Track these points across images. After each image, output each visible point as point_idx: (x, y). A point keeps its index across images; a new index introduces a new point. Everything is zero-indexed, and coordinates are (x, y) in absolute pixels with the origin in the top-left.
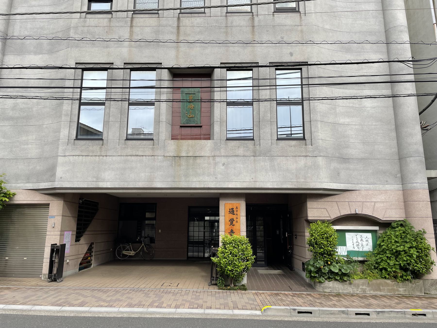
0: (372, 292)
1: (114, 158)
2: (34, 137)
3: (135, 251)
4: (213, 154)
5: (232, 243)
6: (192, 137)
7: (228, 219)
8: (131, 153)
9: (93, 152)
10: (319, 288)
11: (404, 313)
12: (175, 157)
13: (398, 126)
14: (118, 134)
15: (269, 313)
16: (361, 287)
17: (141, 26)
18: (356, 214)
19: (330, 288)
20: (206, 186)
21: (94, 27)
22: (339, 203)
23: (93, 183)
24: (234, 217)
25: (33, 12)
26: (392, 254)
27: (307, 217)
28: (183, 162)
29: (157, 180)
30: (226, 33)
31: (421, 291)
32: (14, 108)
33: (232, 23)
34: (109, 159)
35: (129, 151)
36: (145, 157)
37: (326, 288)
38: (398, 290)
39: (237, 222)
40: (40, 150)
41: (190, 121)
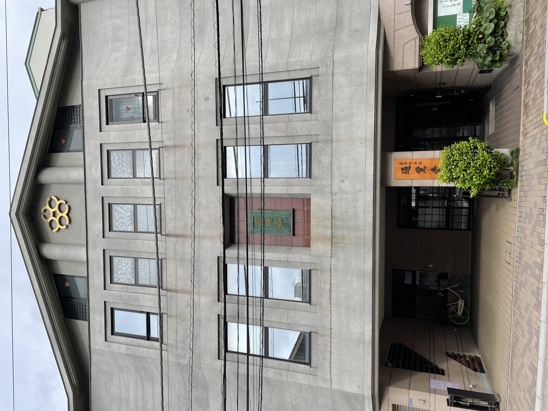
3: (458, 300)
4: (329, 195)
5: (450, 170)
7: (417, 175)
8: (328, 298)
10: (517, 49)
12: (332, 243)
17: (176, 280)
18: (411, 3)
22: (397, 28)
23: (366, 348)
24: (413, 167)
27: (414, 69)
28: (339, 233)
30: (183, 178)
33: (171, 172)
34: (335, 326)
35: (325, 300)
36: (332, 281)
37: (516, 39)
39: (420, 163)
41: (287, 223)
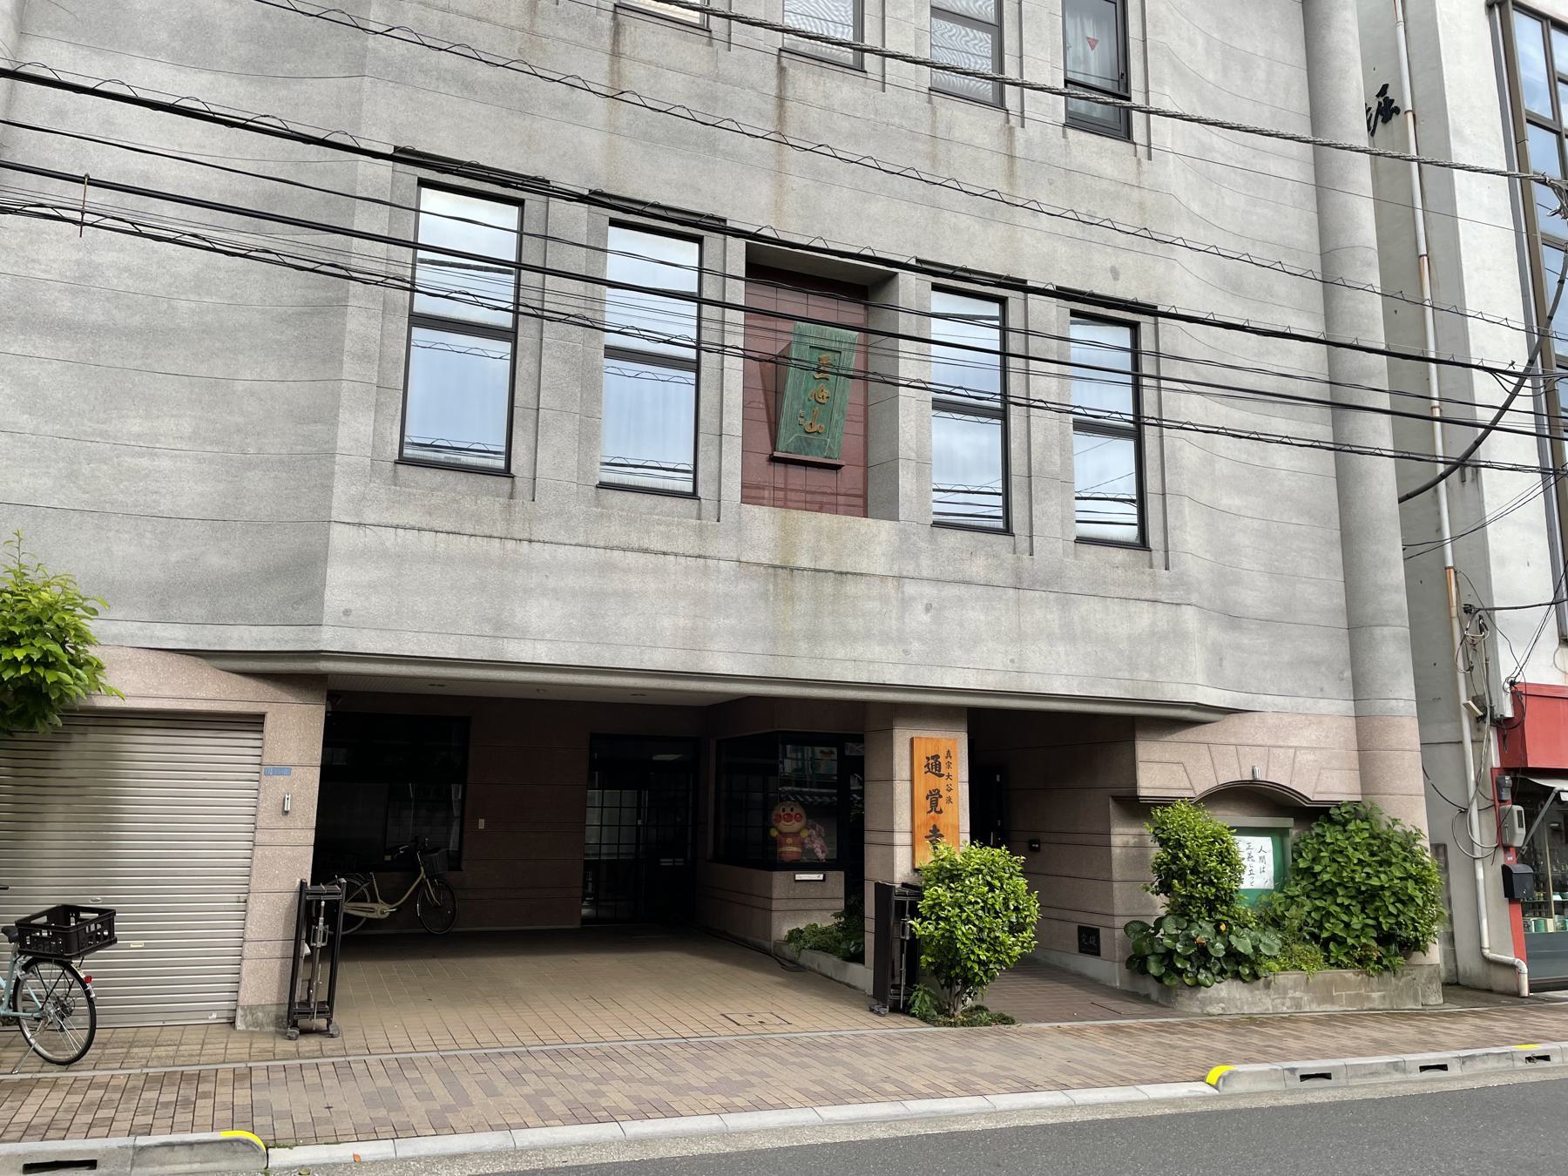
0: (1314, 1007)
1: (561, 551)
2: (187, 427)
3: (389, 901)
4: (895, 571)
5: (979, 871)
6: (809, 497)
7: (921, 793)
8: (621, 540)
9: (479, 522)
10: (1191, 1004)
11: (1511, 1056)
12: (775, 567)
13: (1350, 536)
14: (572, 463)
15: (1237, 1087)
16: (1291, 994)
17: (650, 63)
18: (1254, 781)
19: (1221, 1000)
20: (876, 679)
21: (469, 16)
22: (1213, 748)
23: (480, 641)
24: (941, 784)
25: (1236, 123)
26: (1351, 897)
27: (1134, 786)
28: (802, 586)
29: (716, 647)
30: (934, 159)
31: (1416, 1000)
32: (80, 283)
33: (950, 129)
34: (541, 553)
35: (615, 531)
36: (672, 558)
37: (1211, 1001)
38: (1368, 998)
39: (949, 800)
40: (221, 487)
41: (809, 445)
